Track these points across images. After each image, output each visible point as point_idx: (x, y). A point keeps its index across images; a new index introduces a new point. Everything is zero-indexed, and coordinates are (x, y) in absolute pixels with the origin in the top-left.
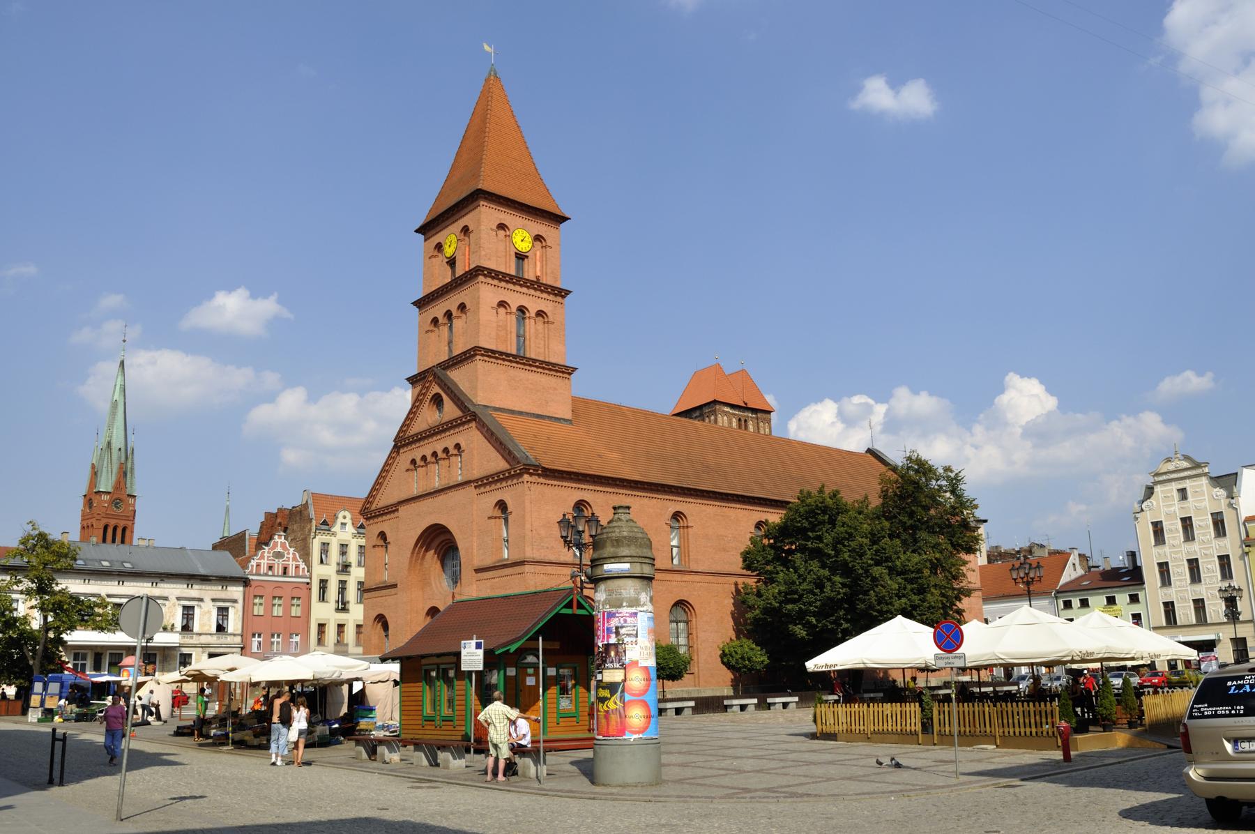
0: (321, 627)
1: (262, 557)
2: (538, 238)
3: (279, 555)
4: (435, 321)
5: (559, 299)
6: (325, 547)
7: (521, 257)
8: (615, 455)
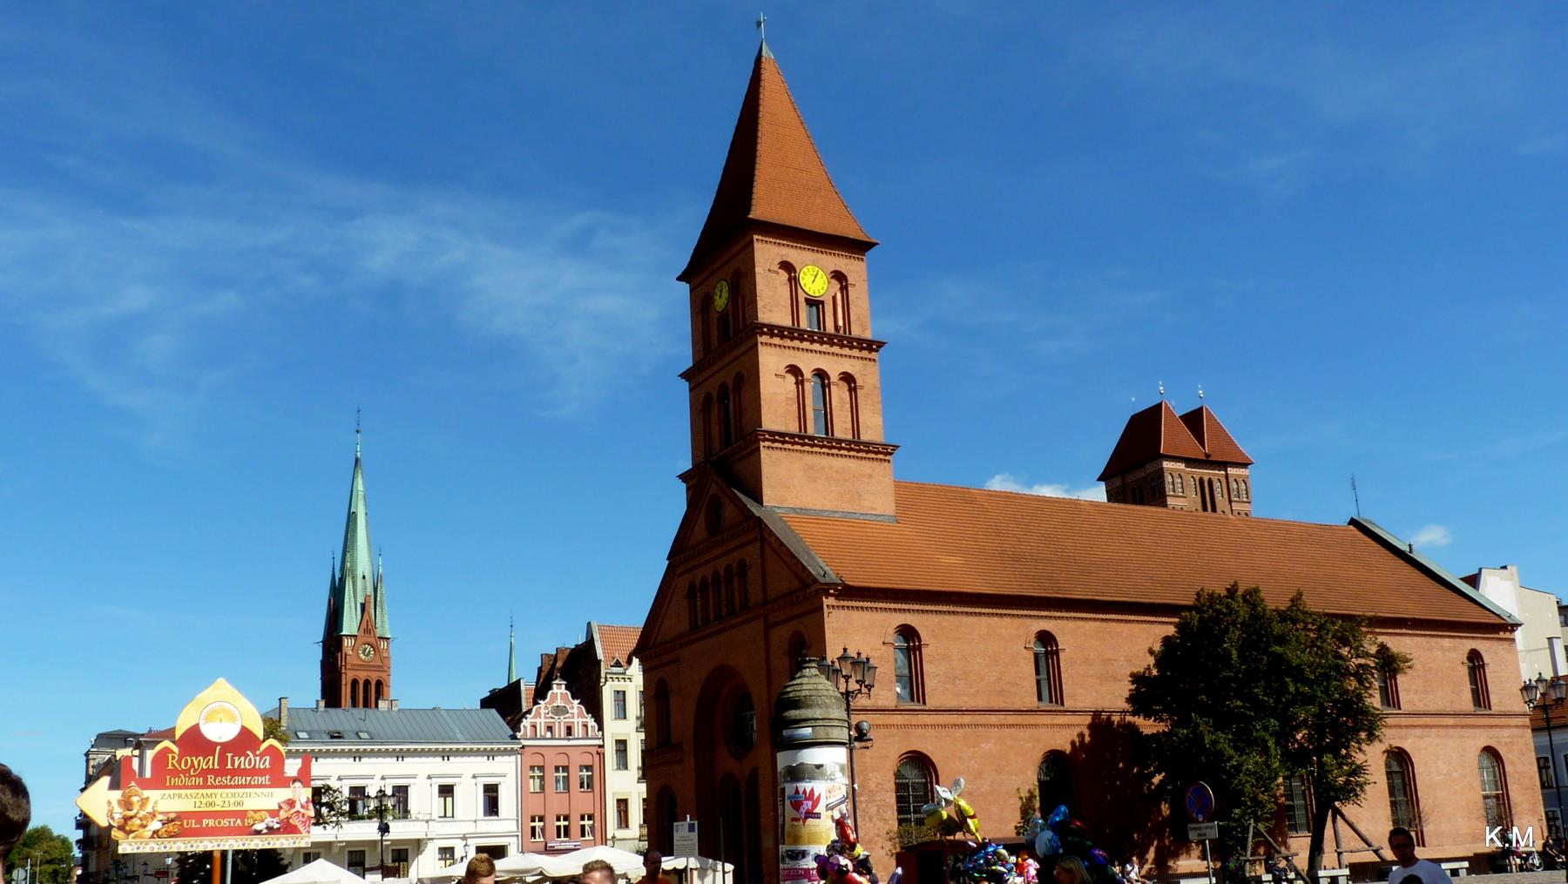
0: (623, 804)
1: (538, 715)
2: (839, 276)
3: (559, 711)
4: (708, 397)
5: (874, 355)
6: (621, 696)
7: (813, 303)
8: (953, 560)
